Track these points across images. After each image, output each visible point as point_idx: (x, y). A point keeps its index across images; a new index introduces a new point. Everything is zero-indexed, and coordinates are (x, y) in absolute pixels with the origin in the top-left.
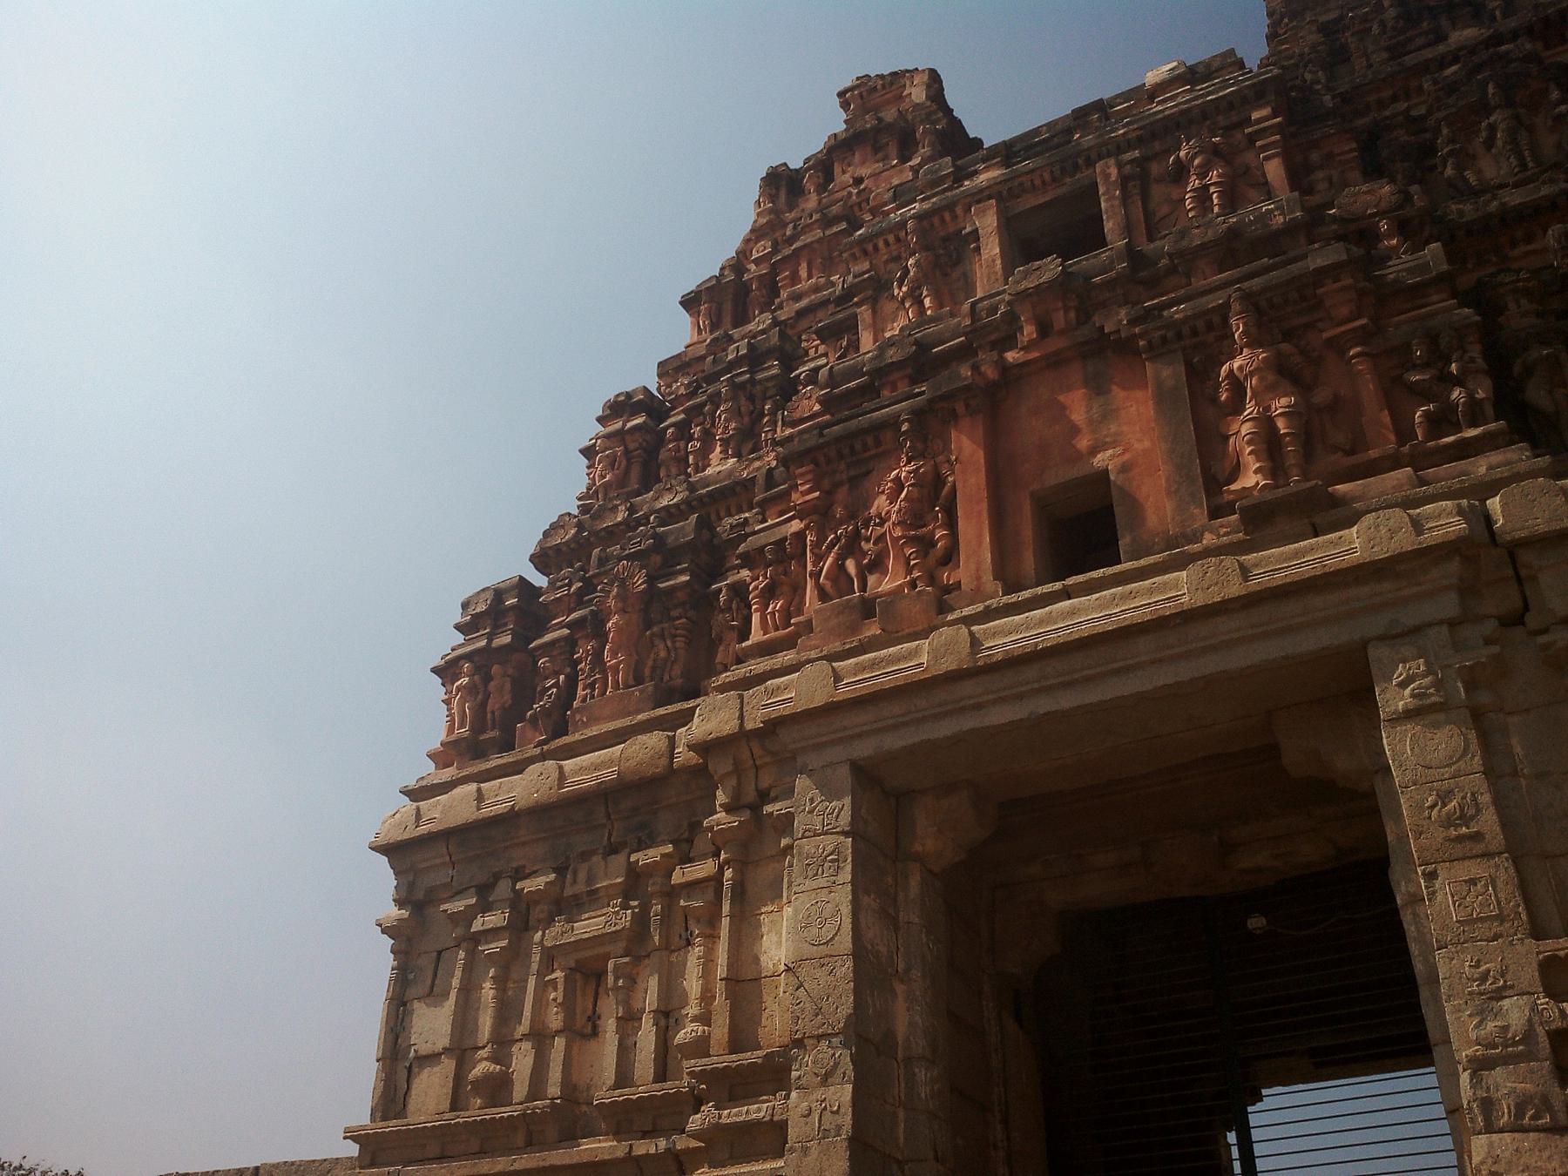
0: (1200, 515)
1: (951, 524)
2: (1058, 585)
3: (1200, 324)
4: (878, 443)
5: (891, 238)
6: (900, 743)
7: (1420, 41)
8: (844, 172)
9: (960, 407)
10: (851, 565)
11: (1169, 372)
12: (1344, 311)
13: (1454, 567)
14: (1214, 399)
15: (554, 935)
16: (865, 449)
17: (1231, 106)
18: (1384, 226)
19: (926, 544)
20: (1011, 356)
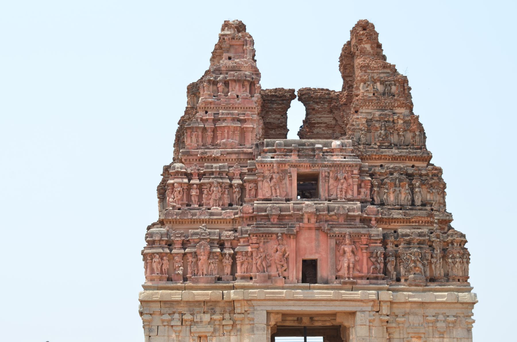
0: (334, 277)
1: (287, 262)
2: (307, 285)
3: (340, 236)
4: (272, 236)
5: (269, 165)
6: (276, 309)
7: (386, 144)
8: (233, 90)
9: (292, 237)
10: (264, 263)
11: (333, 242)
12: (365, 243)
13: (372, 303)
14: (339, 251)
15: (194, 329)
16: (269, 237)
17: (350, 166)
18: (373, 219)
19: (283, 266)
20: (301, 224)
